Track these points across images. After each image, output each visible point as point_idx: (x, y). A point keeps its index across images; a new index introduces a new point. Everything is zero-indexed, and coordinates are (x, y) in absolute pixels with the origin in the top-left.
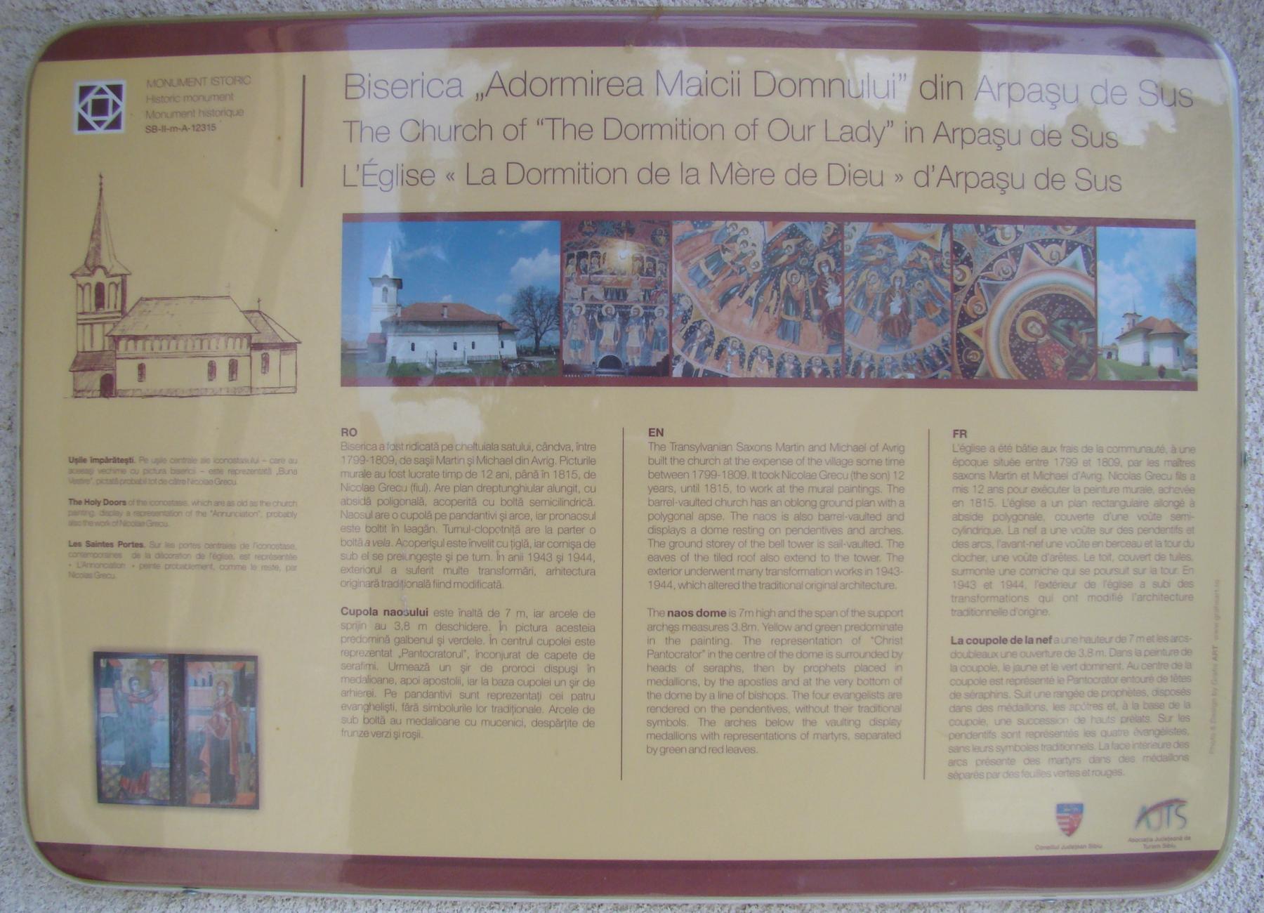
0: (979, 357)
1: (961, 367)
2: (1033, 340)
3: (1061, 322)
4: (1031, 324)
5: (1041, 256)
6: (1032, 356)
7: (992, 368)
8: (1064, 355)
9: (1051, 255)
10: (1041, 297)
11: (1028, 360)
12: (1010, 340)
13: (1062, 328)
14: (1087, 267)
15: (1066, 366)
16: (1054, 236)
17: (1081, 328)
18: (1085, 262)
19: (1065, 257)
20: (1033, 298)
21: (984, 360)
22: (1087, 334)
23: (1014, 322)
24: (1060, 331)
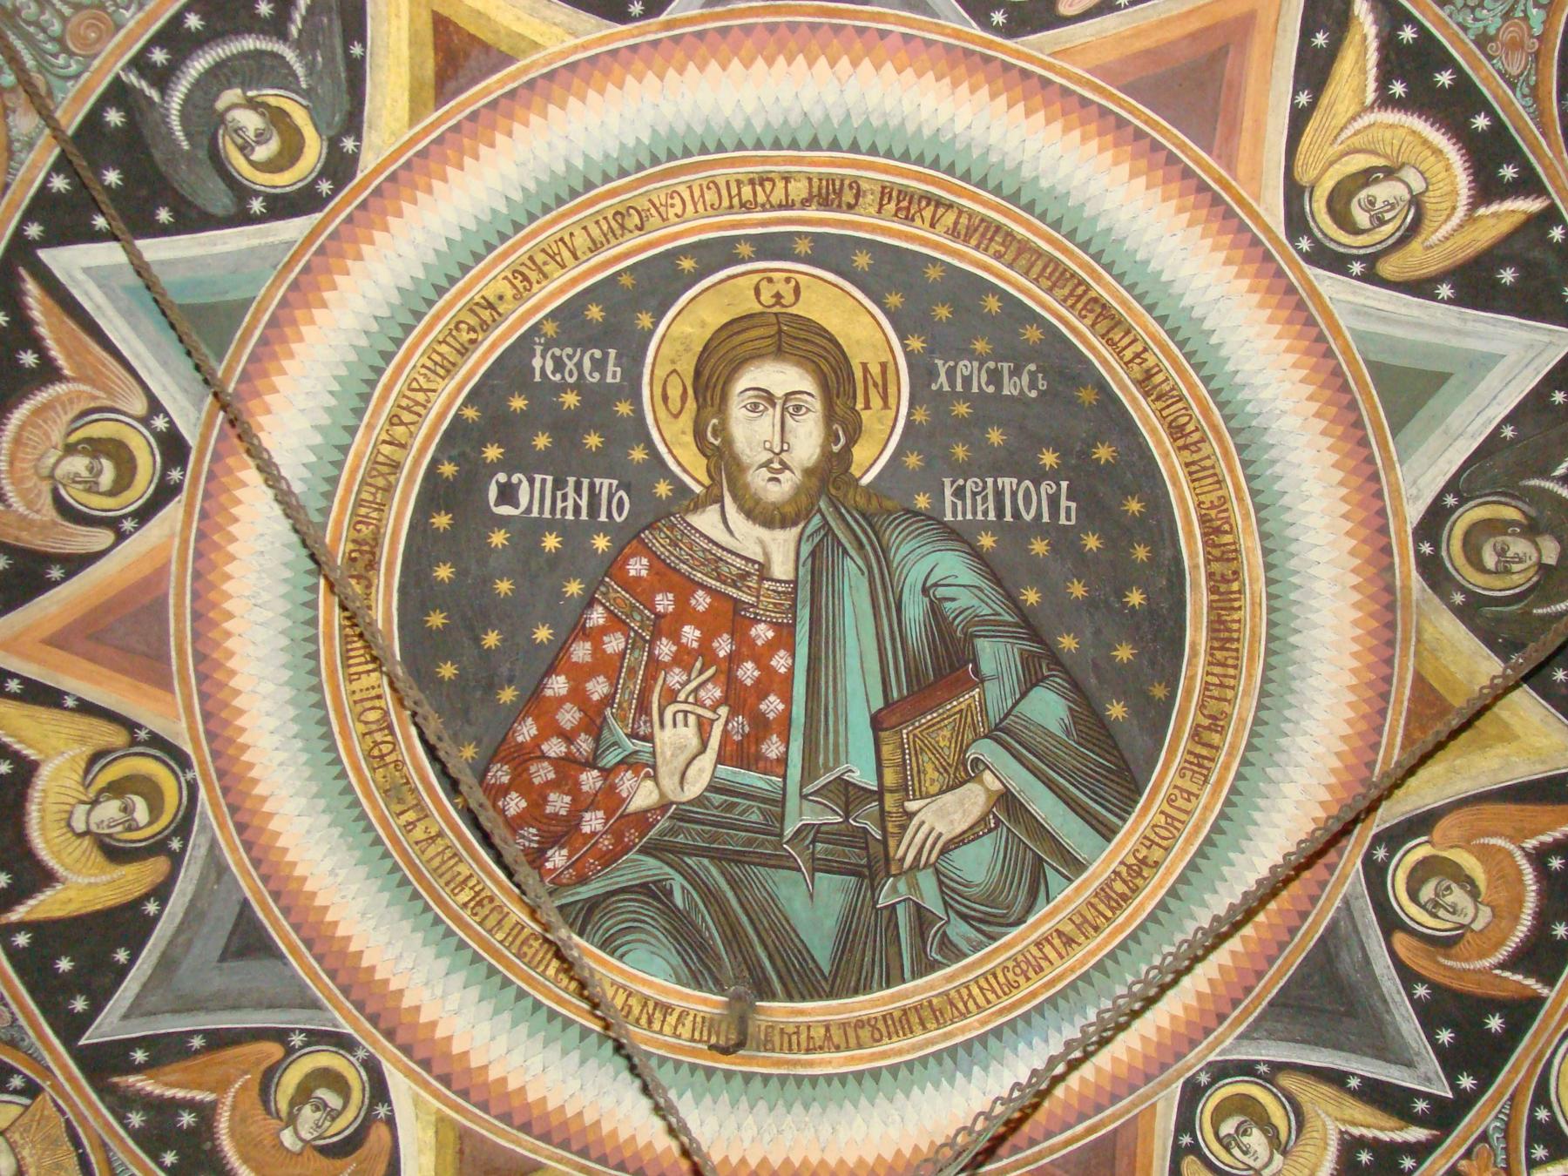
0: (286, 180)
1: (118, 93)
2: (689, 465)
3: (952, 566)
4: (783, 377)
5: (1299, 119)
6: (574, 534)
7: (279, 330)
8: (740, 753)
9: (1366, 177)
10: (1017, 312)
11: (529, 530)
12: (569, 314)
13: (915, 609)
14: (1461, 486)
15: (683, 815)
16: (1515, 109)
17: (1003, 732)
18: (1491, 446)
19: (1420, 288)
20: (973, 260)
21: (294, 229)
22: (1007, 802)
23: (716, 254)
24: (886, 599)
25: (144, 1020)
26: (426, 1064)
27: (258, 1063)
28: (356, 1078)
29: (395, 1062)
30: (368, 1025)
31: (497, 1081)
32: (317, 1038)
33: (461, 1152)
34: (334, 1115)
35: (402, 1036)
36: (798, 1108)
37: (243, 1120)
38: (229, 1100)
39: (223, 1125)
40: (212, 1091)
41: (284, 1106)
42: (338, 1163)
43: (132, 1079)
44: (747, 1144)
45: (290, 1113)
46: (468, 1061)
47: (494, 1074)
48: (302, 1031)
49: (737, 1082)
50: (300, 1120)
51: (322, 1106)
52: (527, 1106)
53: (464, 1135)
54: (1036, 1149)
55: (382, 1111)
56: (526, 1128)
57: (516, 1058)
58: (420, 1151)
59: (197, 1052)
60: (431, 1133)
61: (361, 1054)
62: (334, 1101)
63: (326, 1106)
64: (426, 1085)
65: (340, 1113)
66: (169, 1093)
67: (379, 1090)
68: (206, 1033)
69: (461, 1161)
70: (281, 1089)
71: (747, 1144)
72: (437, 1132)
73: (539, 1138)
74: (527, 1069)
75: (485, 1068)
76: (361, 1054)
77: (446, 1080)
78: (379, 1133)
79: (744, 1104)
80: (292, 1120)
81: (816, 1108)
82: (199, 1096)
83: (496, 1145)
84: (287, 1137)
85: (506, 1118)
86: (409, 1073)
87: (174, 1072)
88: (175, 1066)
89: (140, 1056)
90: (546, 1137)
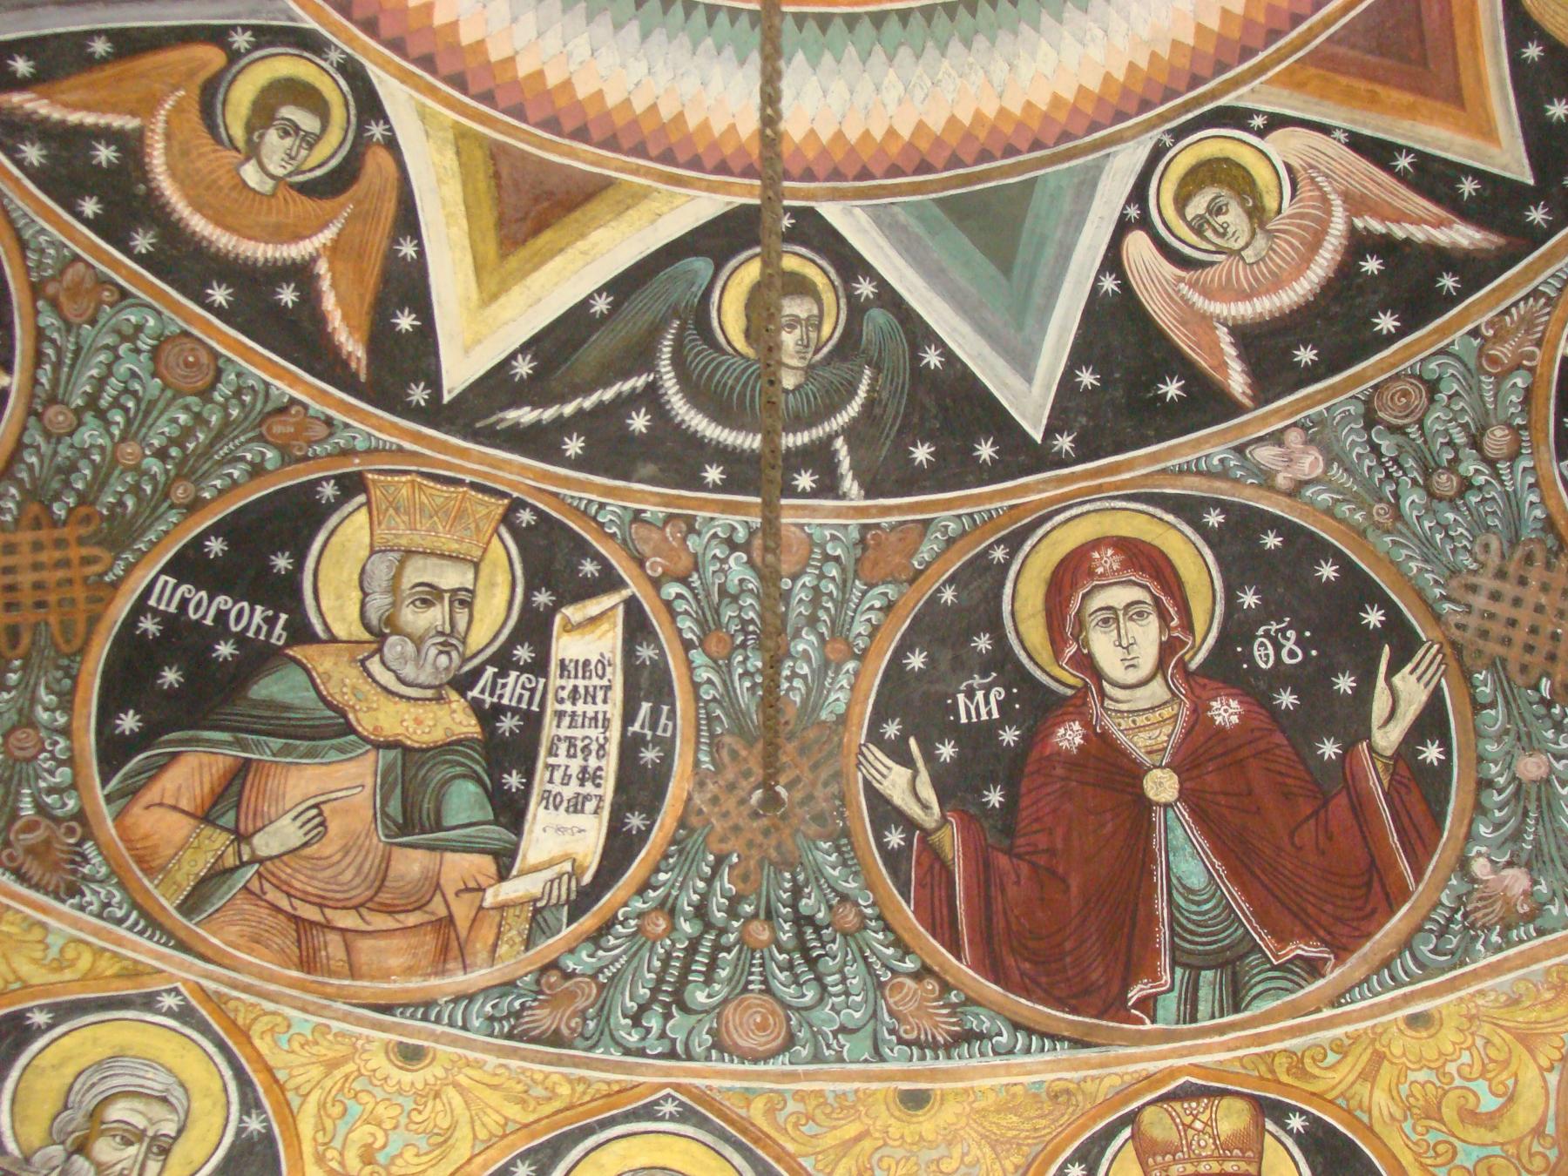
25: (18, 14)
26: (427, 62)
27: (191, 74)
28: (333, 90)
29: (385, 65)
30: (337, 16)
31: (530, 76)
32: (267, 36)
33: (497, 175)
34: (311, 141)
35: (387, 28)
36: (956, 47)
37: (185, 153)
38: (160, 126)
39: (157, 159)
40: (134, 114)
41: (238, 132)
42: (328, 205)
43: (16, 98)
44: (892, 108)
45: (249, 141)
46: (485, 53)
47: (524, 68)
48: (245, 28)
49: (865, 27)
50: (265, 151)
51: (289, 130)
52: (578, 105)
53: (496, 153)
54: (1304, 27)
55: (377, 131)
56: (581, 134)
57: (552, 43)
58: (440, 181)
59: (104, 61)
60: (450, 154)
61: (335, 56)
62: (308, 122)
63: (297, 128)
64: (432, 91)
65: (318, 138)
66: (74, 118)
67: (369, 105)
68: (111, 35)
69: (499, 186)
70: (230, 108)
71: (892, 108)
72: (458, 153)
73: (602, 145)
74: (570, 56)
75: (511, 60)
76: (335, 56)
77: (459, 82)
78: (378, 162)
79: (879, 55)
80: (253, 151)
81: (981, 42)
82: (117, 121)
83: (542, 161)
84: (250, 174)
85: (552, 125)
86: (405, 77)
87: (76, 87)
88: (72, 82)
89: (22, 66)
90: (611, 143)
